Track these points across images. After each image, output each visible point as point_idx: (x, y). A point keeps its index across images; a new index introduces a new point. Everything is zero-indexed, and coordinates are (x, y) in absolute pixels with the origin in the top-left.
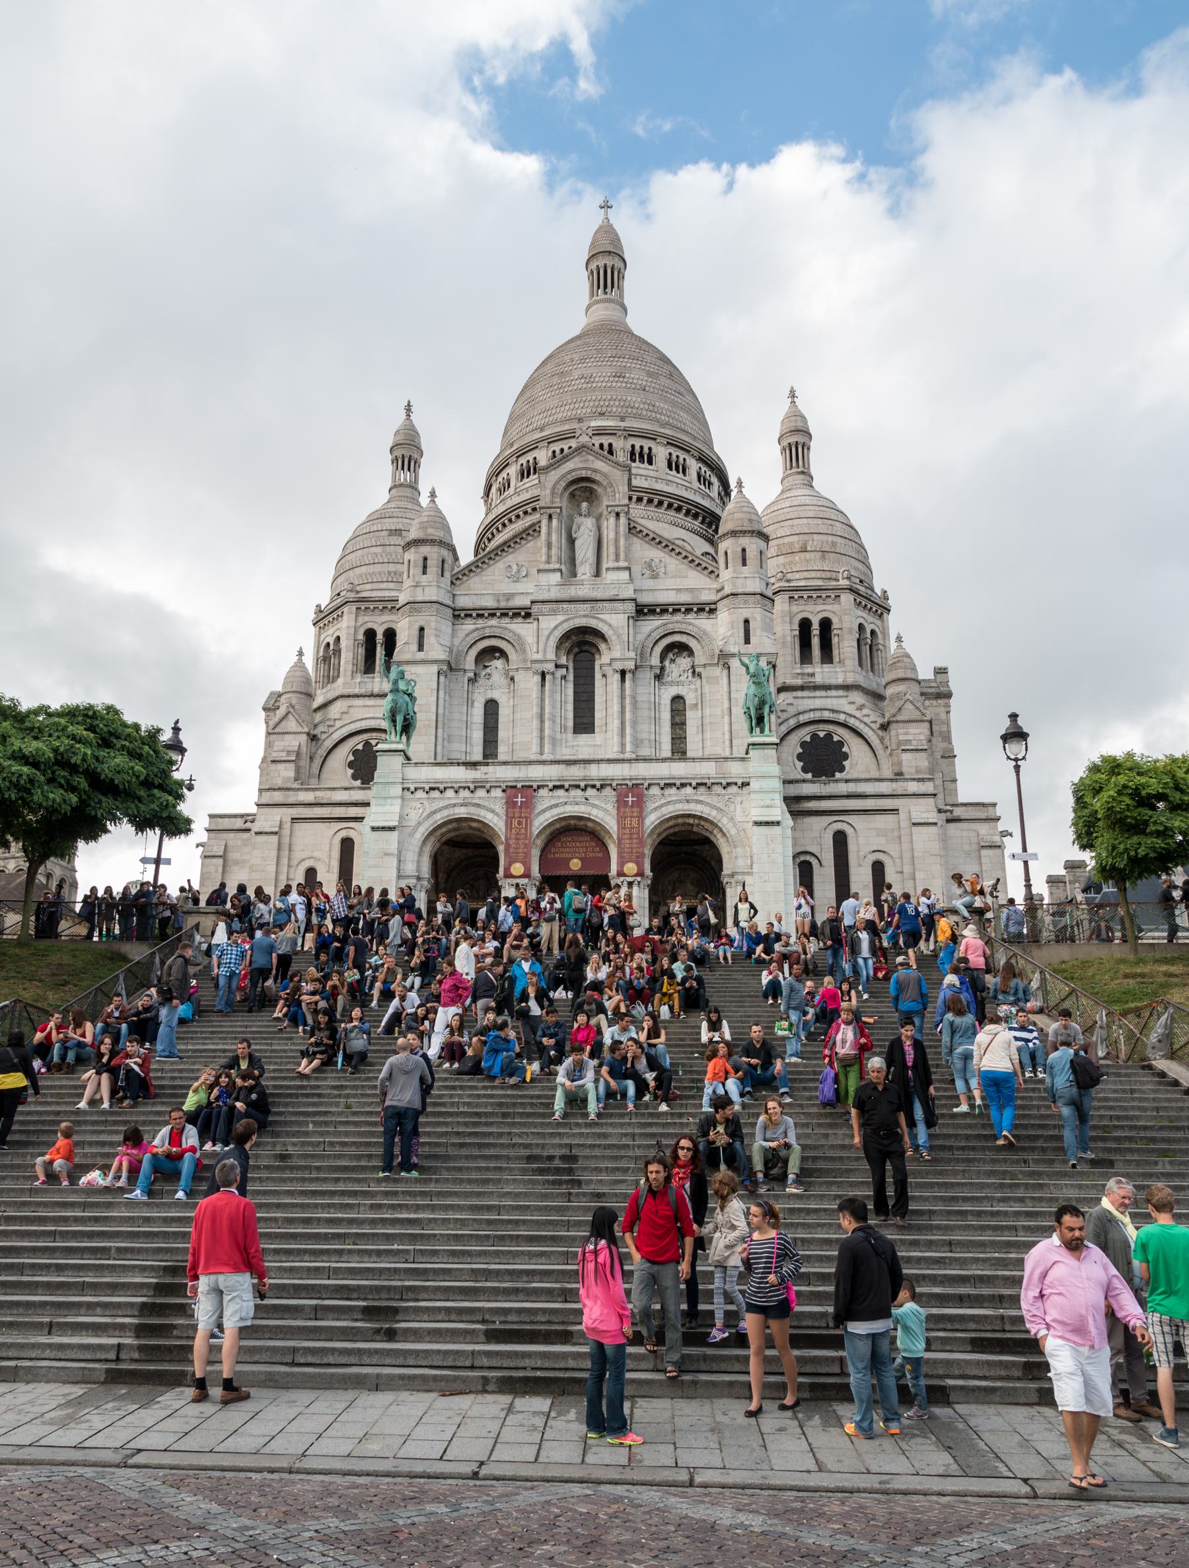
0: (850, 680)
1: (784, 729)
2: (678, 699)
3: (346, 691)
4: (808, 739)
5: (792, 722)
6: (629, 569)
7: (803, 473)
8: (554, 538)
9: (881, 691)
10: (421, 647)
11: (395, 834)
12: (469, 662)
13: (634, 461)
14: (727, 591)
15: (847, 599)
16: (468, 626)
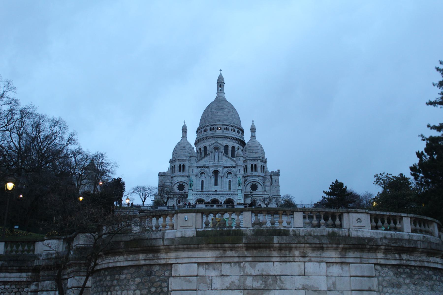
0: (259, 175)
1: (248, 183)
2: (230, 181)
3: (177, 175)
4: (252, 184)
5: (249, 182)
6: (223, 161)
7: (254, 136)
8: (212, 156)
9: (264, 176)
10: (192, 173)
11: (191, 201)
12: (199, 175)
13: (225, 130)
14: (237, 165)
15: (259, 161)
16: (199, 169)
